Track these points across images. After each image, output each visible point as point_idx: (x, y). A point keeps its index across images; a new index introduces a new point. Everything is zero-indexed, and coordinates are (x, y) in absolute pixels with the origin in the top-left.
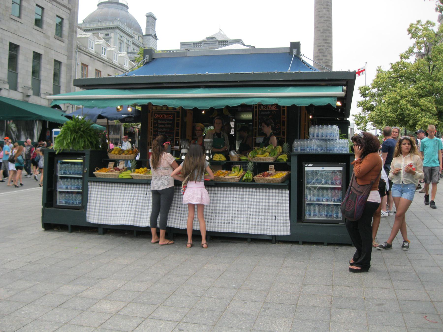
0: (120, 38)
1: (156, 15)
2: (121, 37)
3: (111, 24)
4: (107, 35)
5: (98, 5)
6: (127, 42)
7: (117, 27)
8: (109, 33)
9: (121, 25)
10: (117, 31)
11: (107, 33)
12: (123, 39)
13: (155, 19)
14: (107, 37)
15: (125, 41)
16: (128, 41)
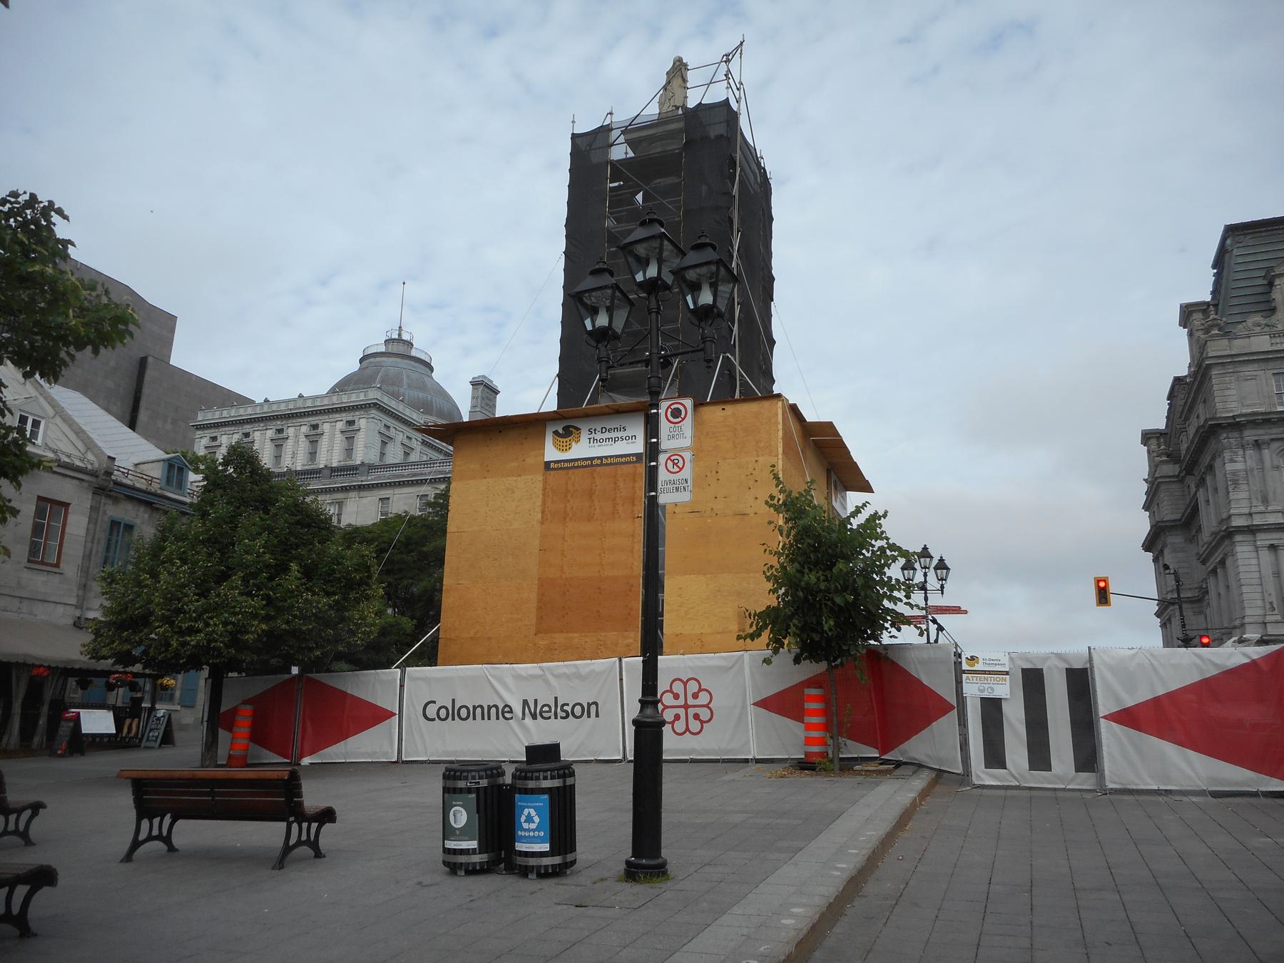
0: (383, 430)
1: (497, 383)
2: (387, 427)
3: (362, 397)
4: (351, 423)
5: (361, 361)
6: (406, 442)
7: (375, 404)
8: (356, 418)
9: (386, 399)
10: (374, 412)
11: (350, 418)
12: (392, 433)
13: (496, 392)
14: (351, 428)
15: (400, 437)
16: (410, 438)
